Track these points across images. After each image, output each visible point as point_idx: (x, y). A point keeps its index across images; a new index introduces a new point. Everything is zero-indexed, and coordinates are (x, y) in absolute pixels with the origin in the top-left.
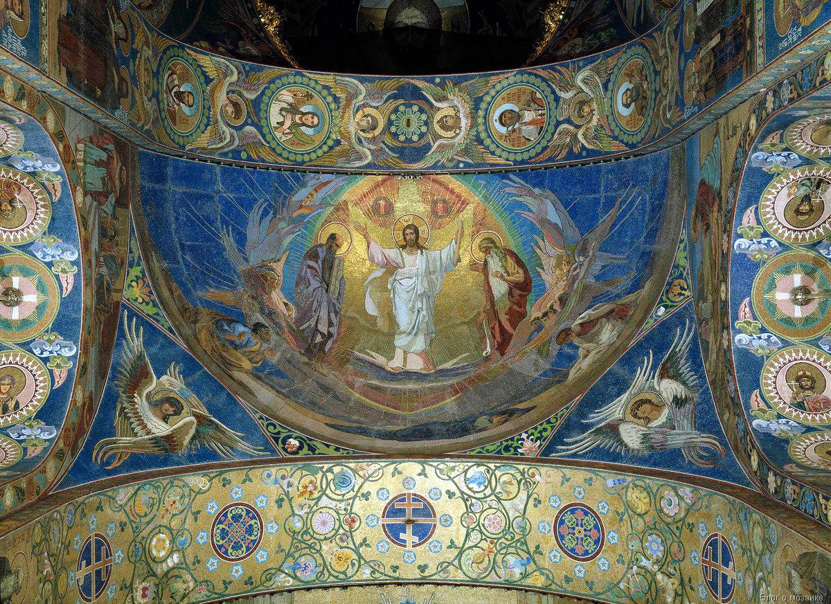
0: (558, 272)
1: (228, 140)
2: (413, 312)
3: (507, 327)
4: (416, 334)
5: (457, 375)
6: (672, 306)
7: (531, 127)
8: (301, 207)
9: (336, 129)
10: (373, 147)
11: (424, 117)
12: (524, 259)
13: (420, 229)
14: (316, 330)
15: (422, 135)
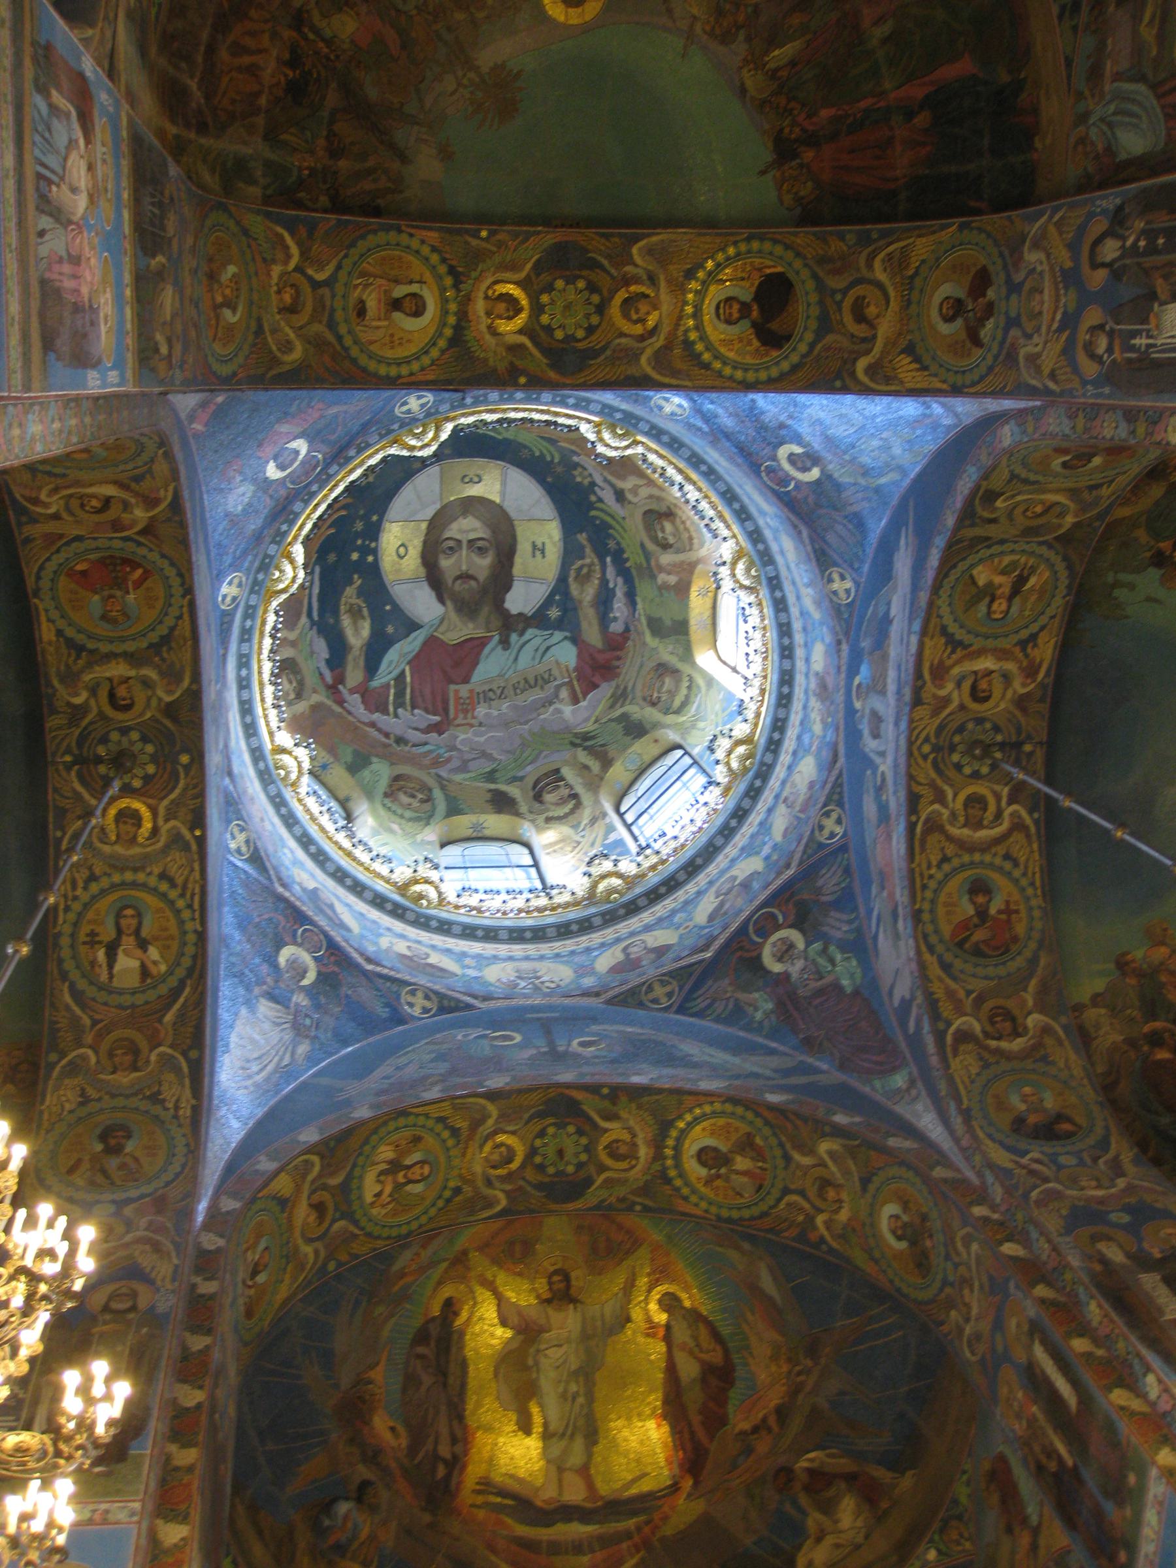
0: (774, 1368)
1: (311, 1260)
2: (566, 1399)
3: (701, 1434)
4: (572, 1436)
5: (634, 1513)
6: (946, 1554)
7: (745, 1179)
8: (402, 1275)
9: (456, 1172)
10: (508, 1187)
11: (584, 1141)
12: (725, 1331)
13: (573, 1275)
14: (436, 1458)
15: (580, 1166)
